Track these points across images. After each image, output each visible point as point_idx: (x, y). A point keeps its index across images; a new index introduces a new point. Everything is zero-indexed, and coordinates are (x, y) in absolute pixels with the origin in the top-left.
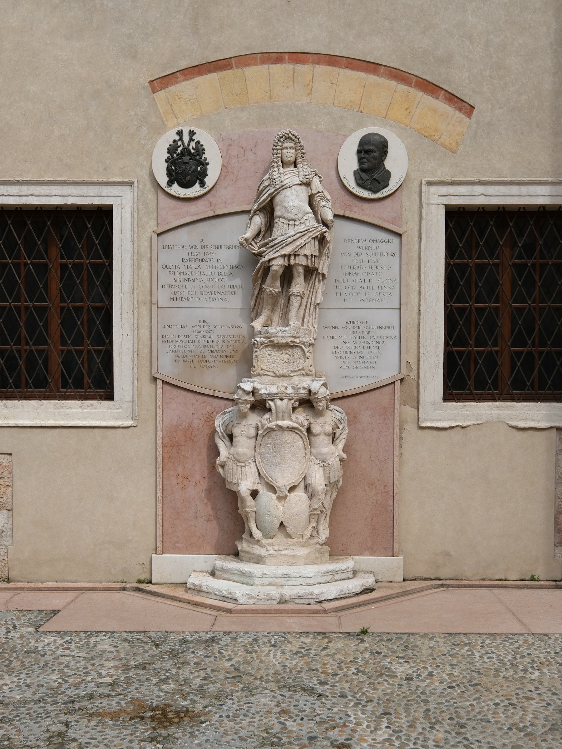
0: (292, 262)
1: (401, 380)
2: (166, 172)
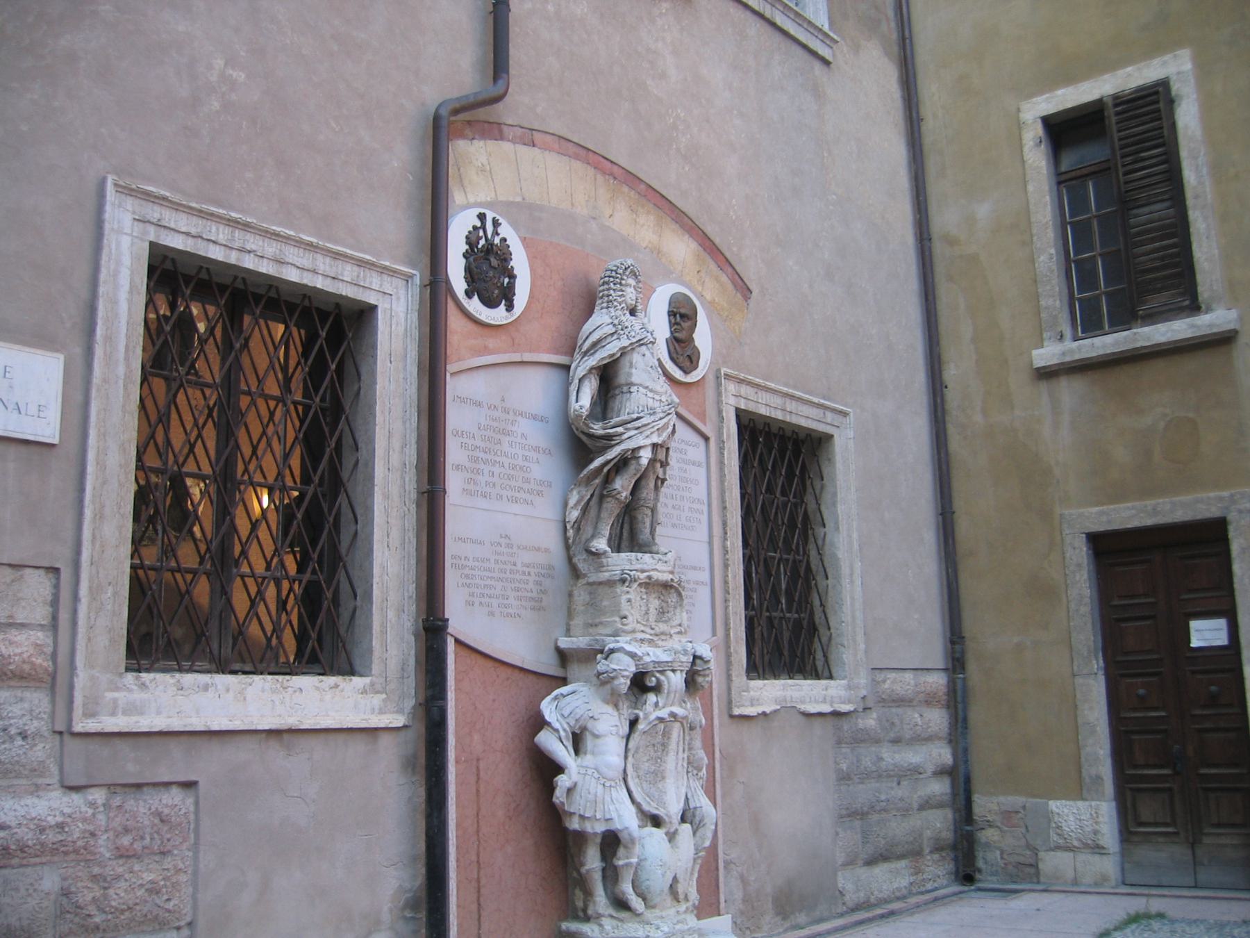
2: (463, 274)
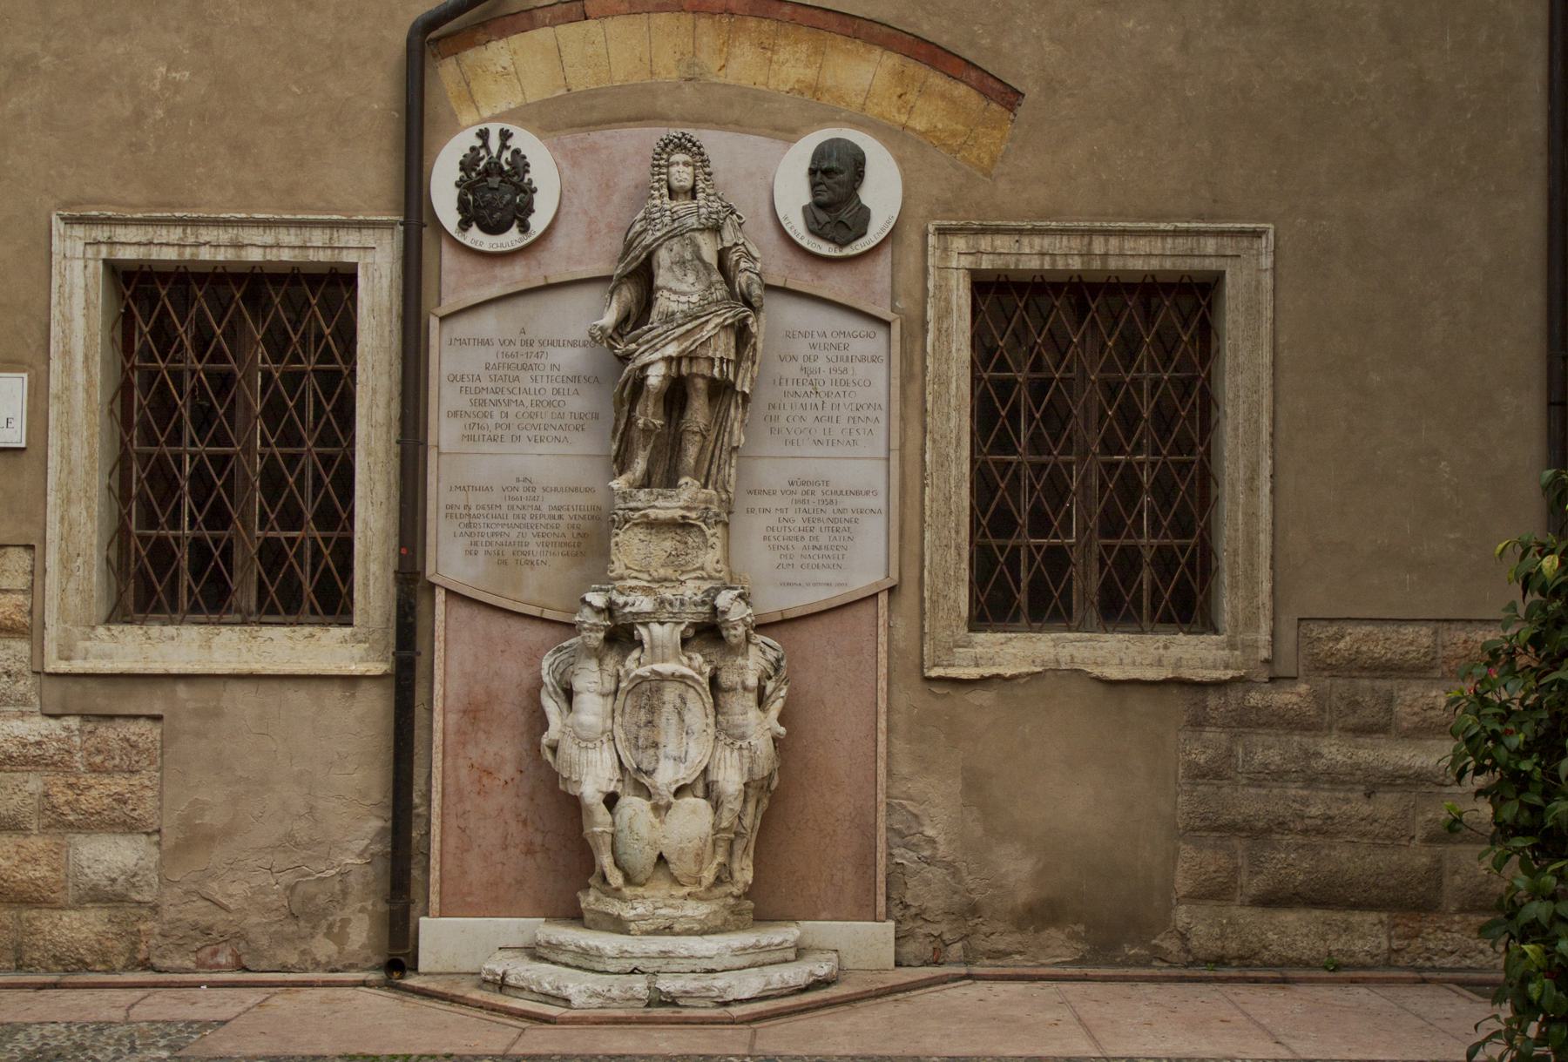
0: (684, 370)
1: (891, 590)
2: (455, 204)
